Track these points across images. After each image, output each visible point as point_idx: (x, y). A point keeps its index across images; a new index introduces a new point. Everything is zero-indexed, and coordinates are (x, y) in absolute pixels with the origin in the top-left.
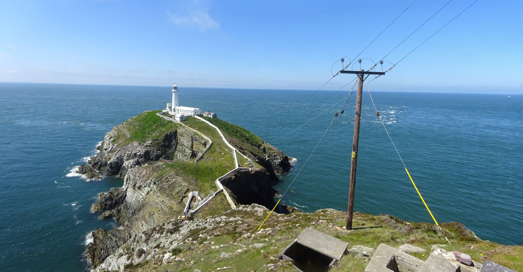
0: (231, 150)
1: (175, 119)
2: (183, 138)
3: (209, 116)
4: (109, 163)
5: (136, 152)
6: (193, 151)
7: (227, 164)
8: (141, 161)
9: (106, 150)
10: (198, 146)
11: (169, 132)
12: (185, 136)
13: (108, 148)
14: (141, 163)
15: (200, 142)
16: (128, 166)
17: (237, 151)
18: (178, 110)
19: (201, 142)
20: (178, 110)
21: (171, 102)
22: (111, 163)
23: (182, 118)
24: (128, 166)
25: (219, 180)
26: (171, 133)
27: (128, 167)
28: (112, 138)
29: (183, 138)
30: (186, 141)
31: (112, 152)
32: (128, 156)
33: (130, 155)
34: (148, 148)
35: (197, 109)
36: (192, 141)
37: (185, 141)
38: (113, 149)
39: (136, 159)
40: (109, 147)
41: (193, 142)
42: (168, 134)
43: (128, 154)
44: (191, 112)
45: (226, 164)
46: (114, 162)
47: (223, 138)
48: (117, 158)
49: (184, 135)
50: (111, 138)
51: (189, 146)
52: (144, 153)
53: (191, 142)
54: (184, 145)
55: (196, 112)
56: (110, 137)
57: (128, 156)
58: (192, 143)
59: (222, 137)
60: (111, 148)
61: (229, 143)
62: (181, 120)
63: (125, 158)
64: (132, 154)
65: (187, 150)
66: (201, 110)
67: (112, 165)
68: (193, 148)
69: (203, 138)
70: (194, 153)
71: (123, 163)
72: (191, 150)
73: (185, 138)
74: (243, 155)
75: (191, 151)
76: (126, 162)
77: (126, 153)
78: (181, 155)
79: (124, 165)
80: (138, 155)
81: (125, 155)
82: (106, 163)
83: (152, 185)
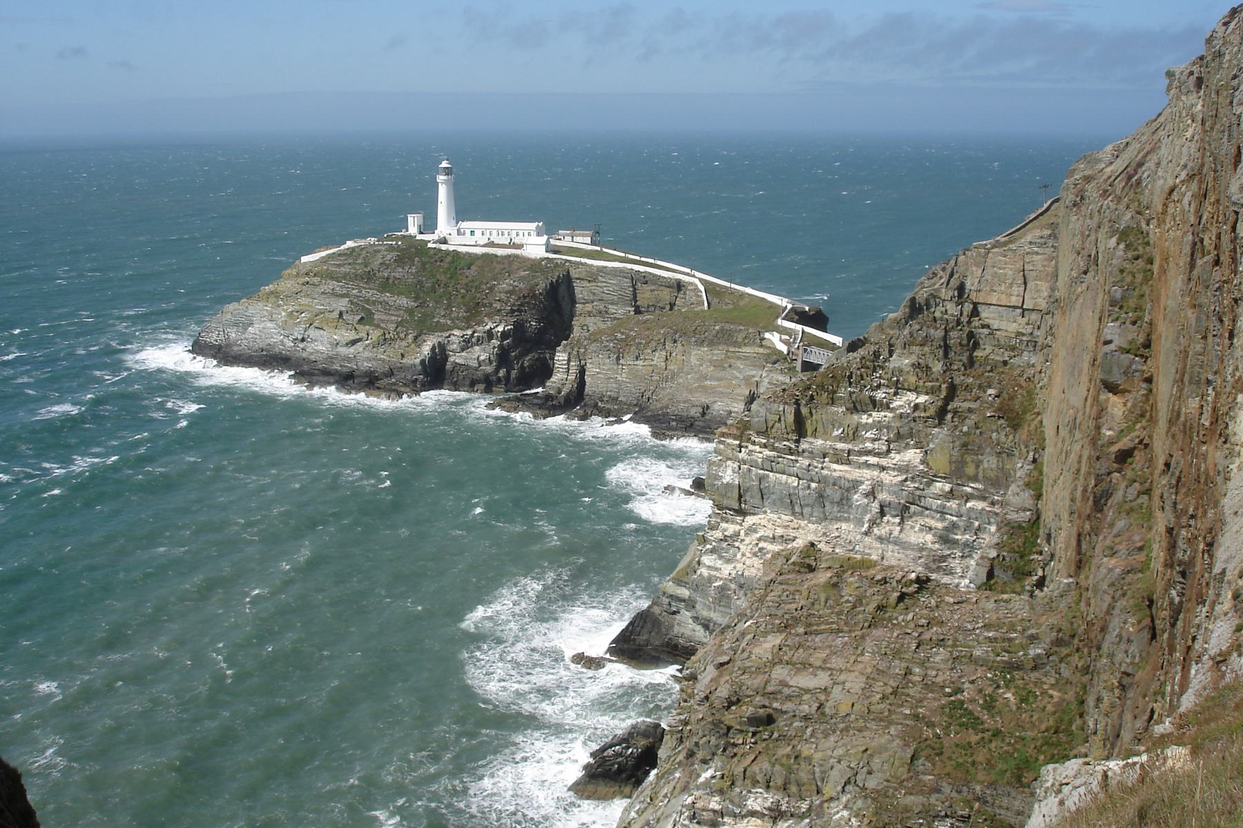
2: (599, 284)
10: (656, 292)
11: (556, 277)
22: (423, 362)
25: (783, 319)
26: (559, 277)
27: (479, 363)
29: (599, 284)
32: (464, 341)
33: (472, 336)
35: (541, 224)
36: (633, 286)
38: (387, 336)
39: (495, 342)
41: (635, 289)
48: (433, 349)
50: (341, 314)
57: (464, 341)
65: (612, 308)
68: (636, 301)
83: (669, 345)
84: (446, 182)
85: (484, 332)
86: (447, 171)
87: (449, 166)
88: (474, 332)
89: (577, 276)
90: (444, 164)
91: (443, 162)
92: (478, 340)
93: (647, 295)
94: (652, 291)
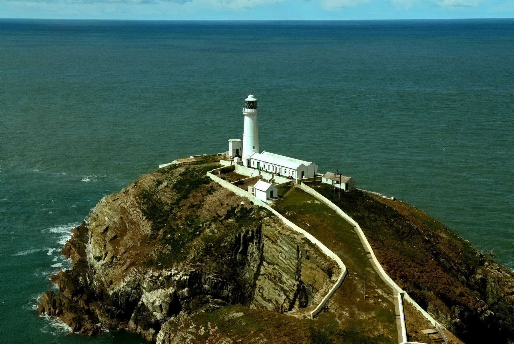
0: (390, 291)
1: (253, 194)
3: (337, 186)
4: (111, 293)
5: (171, 274)
6: (302, 282)
7: (382, 330)
8: (182, 296)
9: (98, 259)
10: (314, 272)
11: (244, 231)
12: (280, 244)
13: (104, 256)
14: (182, 300)
15: (318, 265)
16: (153, 303)
17: (407, 297)
18: (258, 163)
19: (320, 266)
20: (258, 163)
21: (240, 135)
22: (116, 294)
23: (272, 192)
24: (153, 303)
28: (109, 231)
30: (284, 256)
31: (115, 267)
33: (158, 278)
34: (198, 266)
35: (307, 164)
37: (282, 256)
39: (171, 290)
40: (106, 254)
42: (242, 234)
43: (151, 277)
44: (291, 171)
45: (378, 330)
46: (122, 293)
47: (371, 257)
49: (278, 241)
51: (292, 270)
52: (188, 277)
53: (297, 262)
54: (277, 265)
55: (303, 174)
56: (105, 227)
57: (151, 281)
58: (297, 264)
59: (369, 253)
60: (110, 254)
61: (388, 272)
62: (269, 197)
63: (145, 285)
64: (161, 278)
65: (285, 277)
66: (317, 166)
67: (117, 298)
68: (299, 276)
69: (323, 256)
70: (303, 287)
71: (140, 297)
72: (296, 280)
73: (280, 249)
74: (419, 308)
75: (296, 283)
76: (147, 294)
77: (147, 272)
78: (271, 289)
79: (144, 299)
80: (175, 280)
81: (144, 279)
82: (103, 294)
84: (250, 115)
85: (165, 277)
86: (252, 105)
87: (255, 100)
88: (161, 275)
89: (266, 233)
90: (250, 98)
91: (249, 96)
92: (162, 284)
93: (308, 272)
94: (312, 269)
